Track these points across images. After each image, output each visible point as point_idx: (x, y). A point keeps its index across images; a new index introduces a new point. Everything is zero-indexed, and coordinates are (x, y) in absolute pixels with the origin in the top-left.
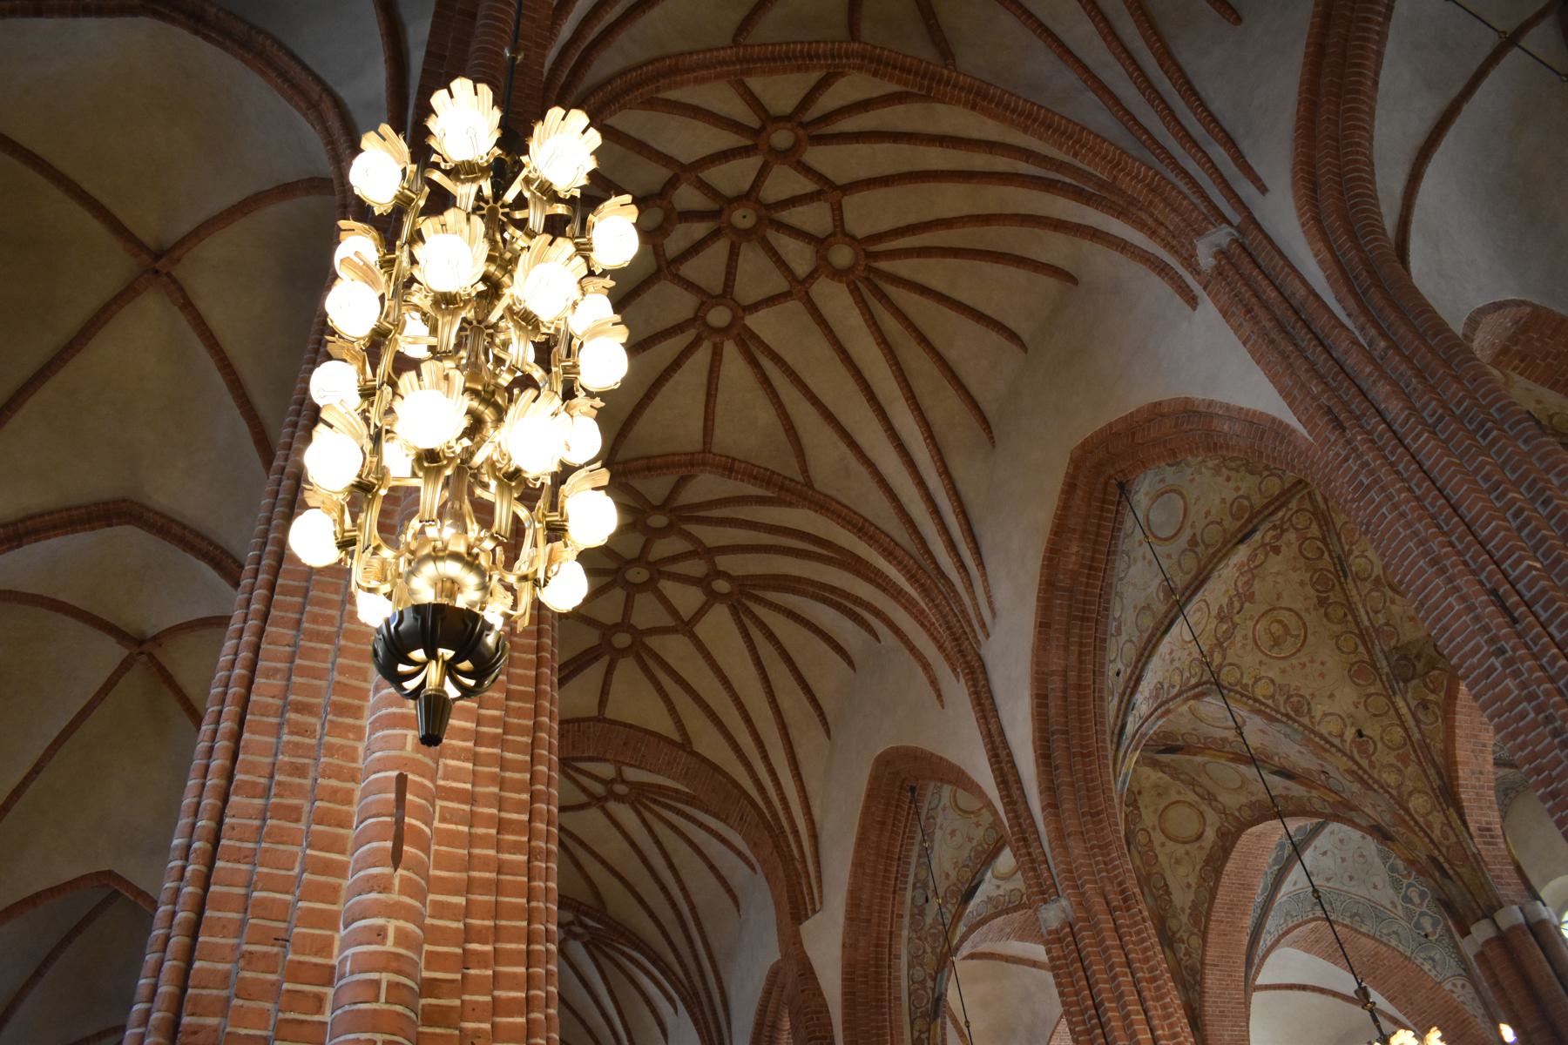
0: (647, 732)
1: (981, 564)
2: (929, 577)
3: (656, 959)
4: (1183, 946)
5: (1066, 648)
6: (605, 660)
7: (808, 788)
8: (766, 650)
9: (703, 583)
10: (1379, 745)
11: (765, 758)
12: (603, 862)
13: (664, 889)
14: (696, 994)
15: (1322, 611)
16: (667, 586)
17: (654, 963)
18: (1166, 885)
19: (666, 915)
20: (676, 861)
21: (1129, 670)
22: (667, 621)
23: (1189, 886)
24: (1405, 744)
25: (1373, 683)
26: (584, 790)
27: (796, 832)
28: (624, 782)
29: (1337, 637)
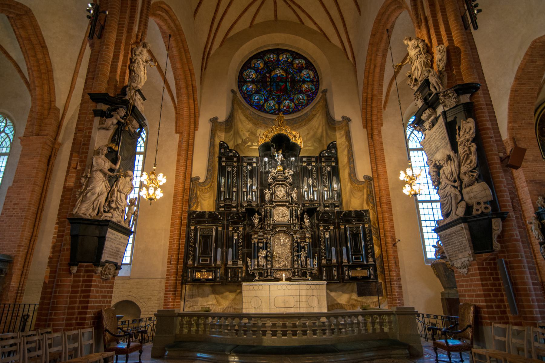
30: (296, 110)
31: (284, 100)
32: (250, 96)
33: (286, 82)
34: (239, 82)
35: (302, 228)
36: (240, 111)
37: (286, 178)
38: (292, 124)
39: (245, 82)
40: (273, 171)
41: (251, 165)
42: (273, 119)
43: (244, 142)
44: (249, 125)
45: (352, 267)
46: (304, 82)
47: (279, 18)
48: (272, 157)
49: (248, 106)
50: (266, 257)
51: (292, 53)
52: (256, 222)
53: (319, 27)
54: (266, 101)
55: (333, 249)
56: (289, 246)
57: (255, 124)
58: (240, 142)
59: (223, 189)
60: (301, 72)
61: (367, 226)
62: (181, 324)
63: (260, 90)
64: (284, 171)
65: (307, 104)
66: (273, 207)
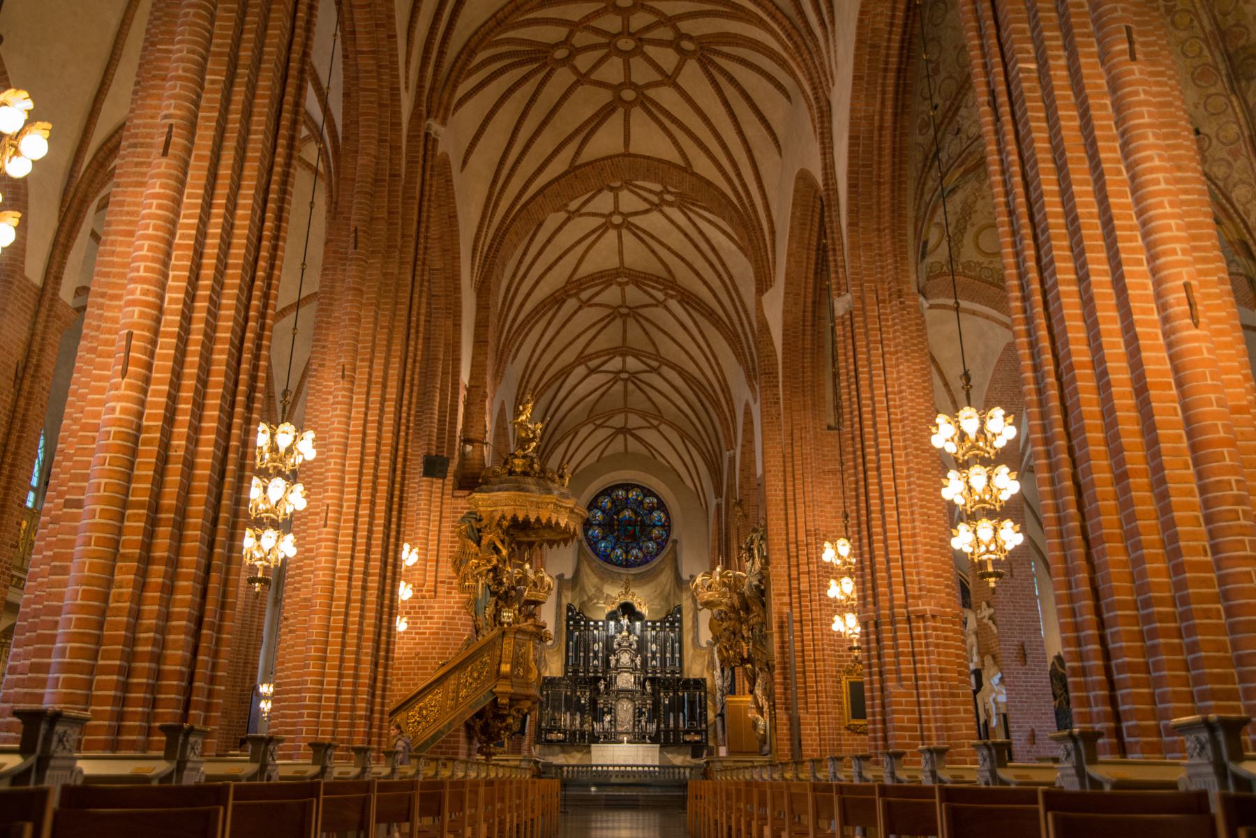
0: (660, 161)
1: (833, 22)
2: (801, 35)
5: (874, 97)
6: (620, 111)
7: (769, 196)
8: (730, 92)
9: (674, 44)
10: (1215, 142)
11: (739, 175)
12: (669, 249)
13: (712, 265)
14: (738, 337)
15: (1169, 19)
16: (650, 50)
19: (716, 283)
21: (948, 103)
22: (657, 77)
24: (1238, 139)
25: (1215, 84)
26: (645, 199)
27: (761, 229)
29: (1183, 43)
30: (645, 561)
32: (596, 543)
38: (641, 579)
40: (619, 636)
41: (597, 628)
43: (590, 599)
44: (595, 580)
45: (687, 732)
46: (654, 526)
48: (618, 621)
49: (594, 557)
50: (610, 722)
51: (642, 488)
52: (602, 687)
54: (613, 549)
56: (631, 711)
57: (601, 579)
58: (585, 598)
65: (657, 554)
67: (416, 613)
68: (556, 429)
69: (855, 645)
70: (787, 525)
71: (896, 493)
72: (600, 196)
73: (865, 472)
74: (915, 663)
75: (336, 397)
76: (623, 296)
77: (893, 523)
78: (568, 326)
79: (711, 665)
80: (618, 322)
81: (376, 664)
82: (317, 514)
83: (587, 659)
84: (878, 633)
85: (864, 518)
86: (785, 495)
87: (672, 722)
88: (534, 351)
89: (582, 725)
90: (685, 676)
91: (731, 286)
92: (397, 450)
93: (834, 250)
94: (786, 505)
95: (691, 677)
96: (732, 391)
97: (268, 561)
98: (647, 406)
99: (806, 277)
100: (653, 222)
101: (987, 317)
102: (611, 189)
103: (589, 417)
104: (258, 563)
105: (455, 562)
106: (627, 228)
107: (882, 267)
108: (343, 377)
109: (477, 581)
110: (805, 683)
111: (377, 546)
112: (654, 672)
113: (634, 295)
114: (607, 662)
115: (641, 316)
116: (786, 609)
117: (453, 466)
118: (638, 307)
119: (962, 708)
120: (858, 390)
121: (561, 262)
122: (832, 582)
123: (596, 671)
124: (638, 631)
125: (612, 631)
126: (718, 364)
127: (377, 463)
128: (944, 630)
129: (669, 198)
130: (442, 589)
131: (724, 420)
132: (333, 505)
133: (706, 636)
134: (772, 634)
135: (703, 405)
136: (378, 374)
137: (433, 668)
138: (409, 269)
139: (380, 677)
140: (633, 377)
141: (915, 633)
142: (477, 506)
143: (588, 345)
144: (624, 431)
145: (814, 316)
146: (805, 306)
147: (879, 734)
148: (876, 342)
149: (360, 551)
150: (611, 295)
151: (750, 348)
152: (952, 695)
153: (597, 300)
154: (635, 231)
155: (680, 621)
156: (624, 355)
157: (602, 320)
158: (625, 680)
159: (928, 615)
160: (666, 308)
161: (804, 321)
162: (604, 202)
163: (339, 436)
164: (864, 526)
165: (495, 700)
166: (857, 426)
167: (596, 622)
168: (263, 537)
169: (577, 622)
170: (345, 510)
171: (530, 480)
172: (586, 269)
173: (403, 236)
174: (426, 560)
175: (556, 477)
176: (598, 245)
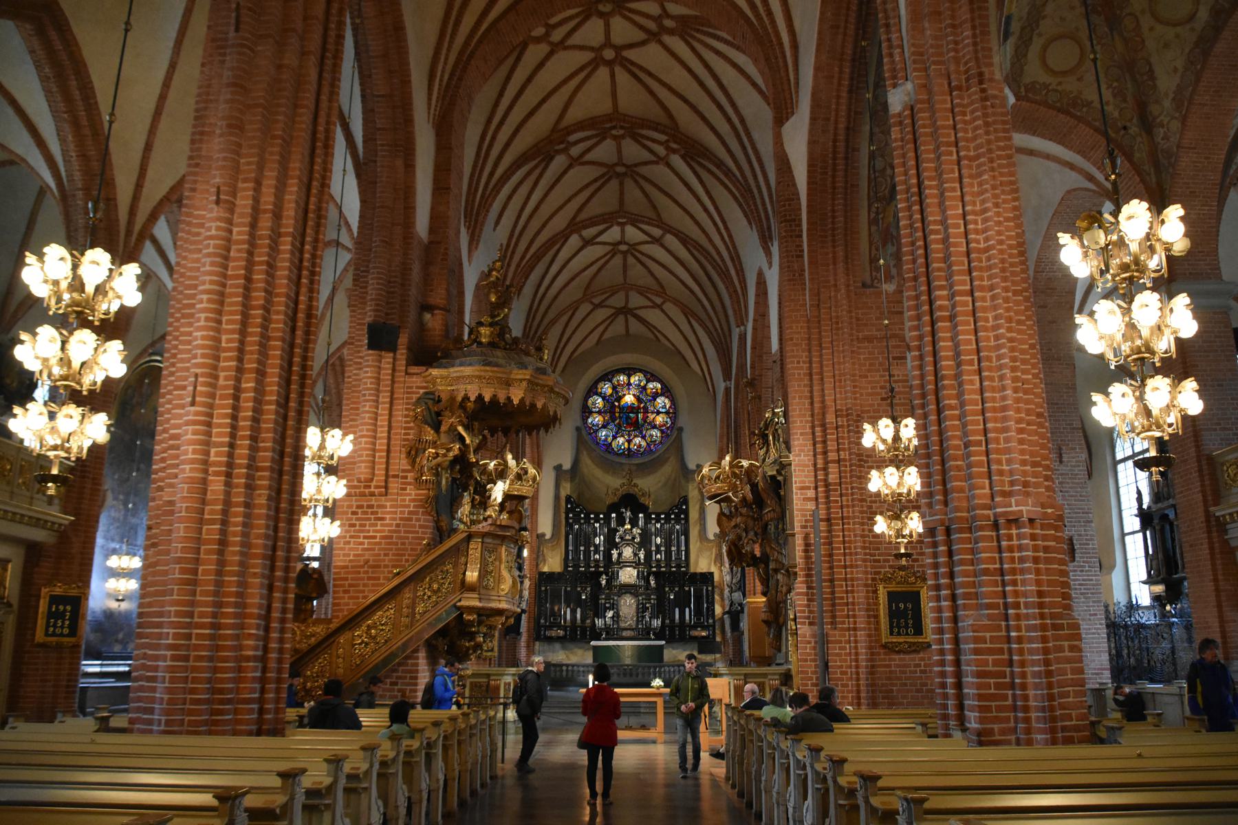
3: (720, 164)
4: (1162, 130)
17: (718, 167)
18: (1151, 71)
19: (724, 128)
20: (725, 82)
23: (1175, 70)
26: (641, 27)
27: (781, 44)
28: (668, 16)
31: (635, 436)
33: (637, 413)
34: (584, 412)
35: (648, 589)
36: (585, 453)
37: (634, 538)
39: (591, 413)
41: (597, 521)
42: (622, 464)
45: (695, 627)
46: (658, 413)
47: (631, 332)
49: (594, 446)
50: (612, 617)
52: (604, 582)
53: (677, 349)
54: (615, 437)
55: (677, 610)
56: (634, 606)
59: (570, 548)
60: (655, 400)
61: (710, 588)
62: (555, 672)
63: (608, 424)
64: (631, 529)
66: (621, 568)
67: (366, 513)
68: (549, 307)
69: (903, 551)
70: (812, 404)
71: (978, 351)
72: (588, 24)
73: (933, 324)
74: (1004, 584)
75: (209, 229)
76: (619, 151)
77: (972, 392)
78: (557, 188)
79: (719, 557)
80: (614, 184)
81: (271, 588)
82: (184, 388)
83: (587, 553)
84: (949, 543)
85: (931, 387)
86: (810, 368)
87: (677, 616)
88: (519, 217)
89: (583, 620)
90: (692, 570)
91: (742, 130)
92: (296, 303)
93: (887, 26)
94: (811, 380)
95: (699, 570)
96: (743, 260)
97: (68, 451)
98: (649, 281)
99: (838, 97)
100: (651, 56)
101: (1048, 157)
102: (601, 15)
103: (585, 295)
104: (51, 454)
105: (409, 453)
106: (624, 67)
107: (956, 43)
108: (218, 202)
109: (437, 475)
110: (833, 593)
111: (268, 430)
112: (658, 566)
113: (632, 151)
114: (608, 555)
115: (638, 174)
116: (811, 506)
117: (403, 340)
118: (636, 165)
119: (1066, 643)
120: (922, 212)
121: (545, 106)
122: (874, 474)
123: (597, 566)
124: (641, 523)
125: (613, 525)
126: (726, 228)
127: (266, 319)
128: (1045, 538)
129: (668, 23)
130: (394, 485)
131: (733, 293)
132: (203, 375)
133: (713, 529)
134: (793, 535)
135: (710, 279)
136: (268, 200)
137: (385, 578)
138: (312, 61)
139: (277, 605)
140: (633, 247)
141: (1004, 543)
142: (434, 384)
143: (580, 210)
144: (625, 311)
145: (847, 147)
146: (836, 134)
147: (950, 680)
148: (948, 144)
149: (243, 438)
150: (605, 151)
151: (764, 204)
152: (1055, 627)
153: (588, 157)
154: (628, 66)
155: (686, 512)
156: (622, 225)
157: (596, 180)
158: (628, 575)
159: (1025, 519)
160: (668, 165)
161: (835, 152)
162: (592, 32)
163: (211, 282)
164: (931, 398)
165: (461, 614)
166: (921, 261)
167: (597, 515)
168: (60, 416)
169: (577, 515)
170: (221, 382)
171: (499, 353)
172: (575, 114)
173: (305, 19)
174: (374, 450)
175: (533, 351)
176: (584, 88)
